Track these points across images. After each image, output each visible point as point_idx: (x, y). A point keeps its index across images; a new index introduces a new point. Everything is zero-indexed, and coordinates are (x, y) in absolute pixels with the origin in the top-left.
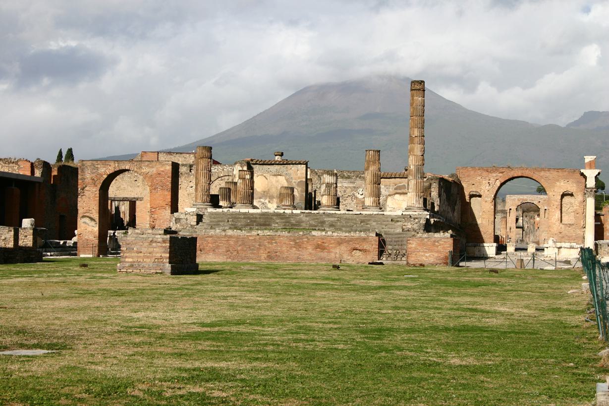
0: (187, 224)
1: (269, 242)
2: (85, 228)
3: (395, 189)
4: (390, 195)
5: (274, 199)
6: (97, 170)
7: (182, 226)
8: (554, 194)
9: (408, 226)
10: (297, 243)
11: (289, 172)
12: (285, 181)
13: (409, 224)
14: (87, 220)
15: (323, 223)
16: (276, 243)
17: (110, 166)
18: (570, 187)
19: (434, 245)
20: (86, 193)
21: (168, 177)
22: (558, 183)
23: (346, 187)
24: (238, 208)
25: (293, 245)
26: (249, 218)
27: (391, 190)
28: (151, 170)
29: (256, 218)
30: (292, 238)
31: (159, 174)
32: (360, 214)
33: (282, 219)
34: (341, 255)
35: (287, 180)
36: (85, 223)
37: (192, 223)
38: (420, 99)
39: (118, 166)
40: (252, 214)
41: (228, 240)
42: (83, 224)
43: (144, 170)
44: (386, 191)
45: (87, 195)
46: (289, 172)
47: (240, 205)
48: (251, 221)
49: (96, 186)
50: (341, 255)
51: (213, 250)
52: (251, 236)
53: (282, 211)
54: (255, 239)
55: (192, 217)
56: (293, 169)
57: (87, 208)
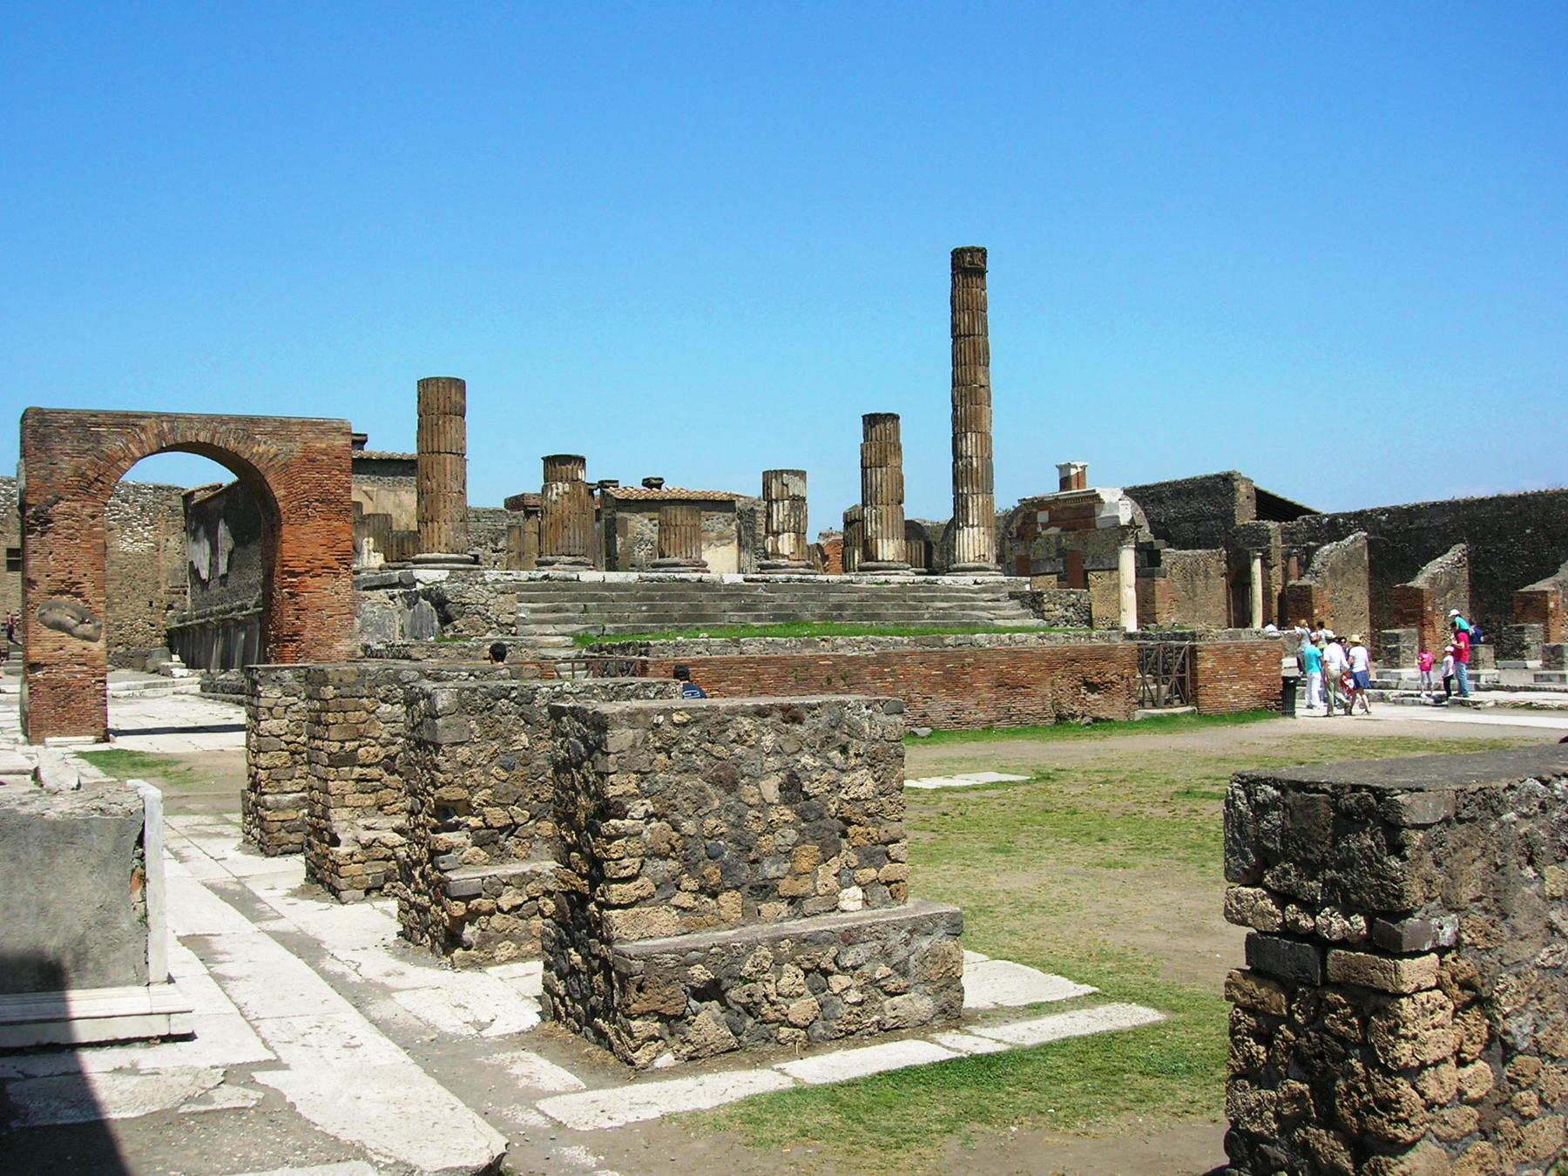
1: (873, 674)
2: (57, 645)
6: (98, 442)
10: (947, 671)
16: (893, 674)
19: (1247, 659)
20: (60, 523)
25: (939, 679)
30: (936, 659)
31: (312, 461)
34: (1056, 704)
36: (58, 626)
39: (172, 430)
50: (1056, 704)
52: (825, 657)
54: (834, 665)
55: (501, 598)
57: (63, 576)
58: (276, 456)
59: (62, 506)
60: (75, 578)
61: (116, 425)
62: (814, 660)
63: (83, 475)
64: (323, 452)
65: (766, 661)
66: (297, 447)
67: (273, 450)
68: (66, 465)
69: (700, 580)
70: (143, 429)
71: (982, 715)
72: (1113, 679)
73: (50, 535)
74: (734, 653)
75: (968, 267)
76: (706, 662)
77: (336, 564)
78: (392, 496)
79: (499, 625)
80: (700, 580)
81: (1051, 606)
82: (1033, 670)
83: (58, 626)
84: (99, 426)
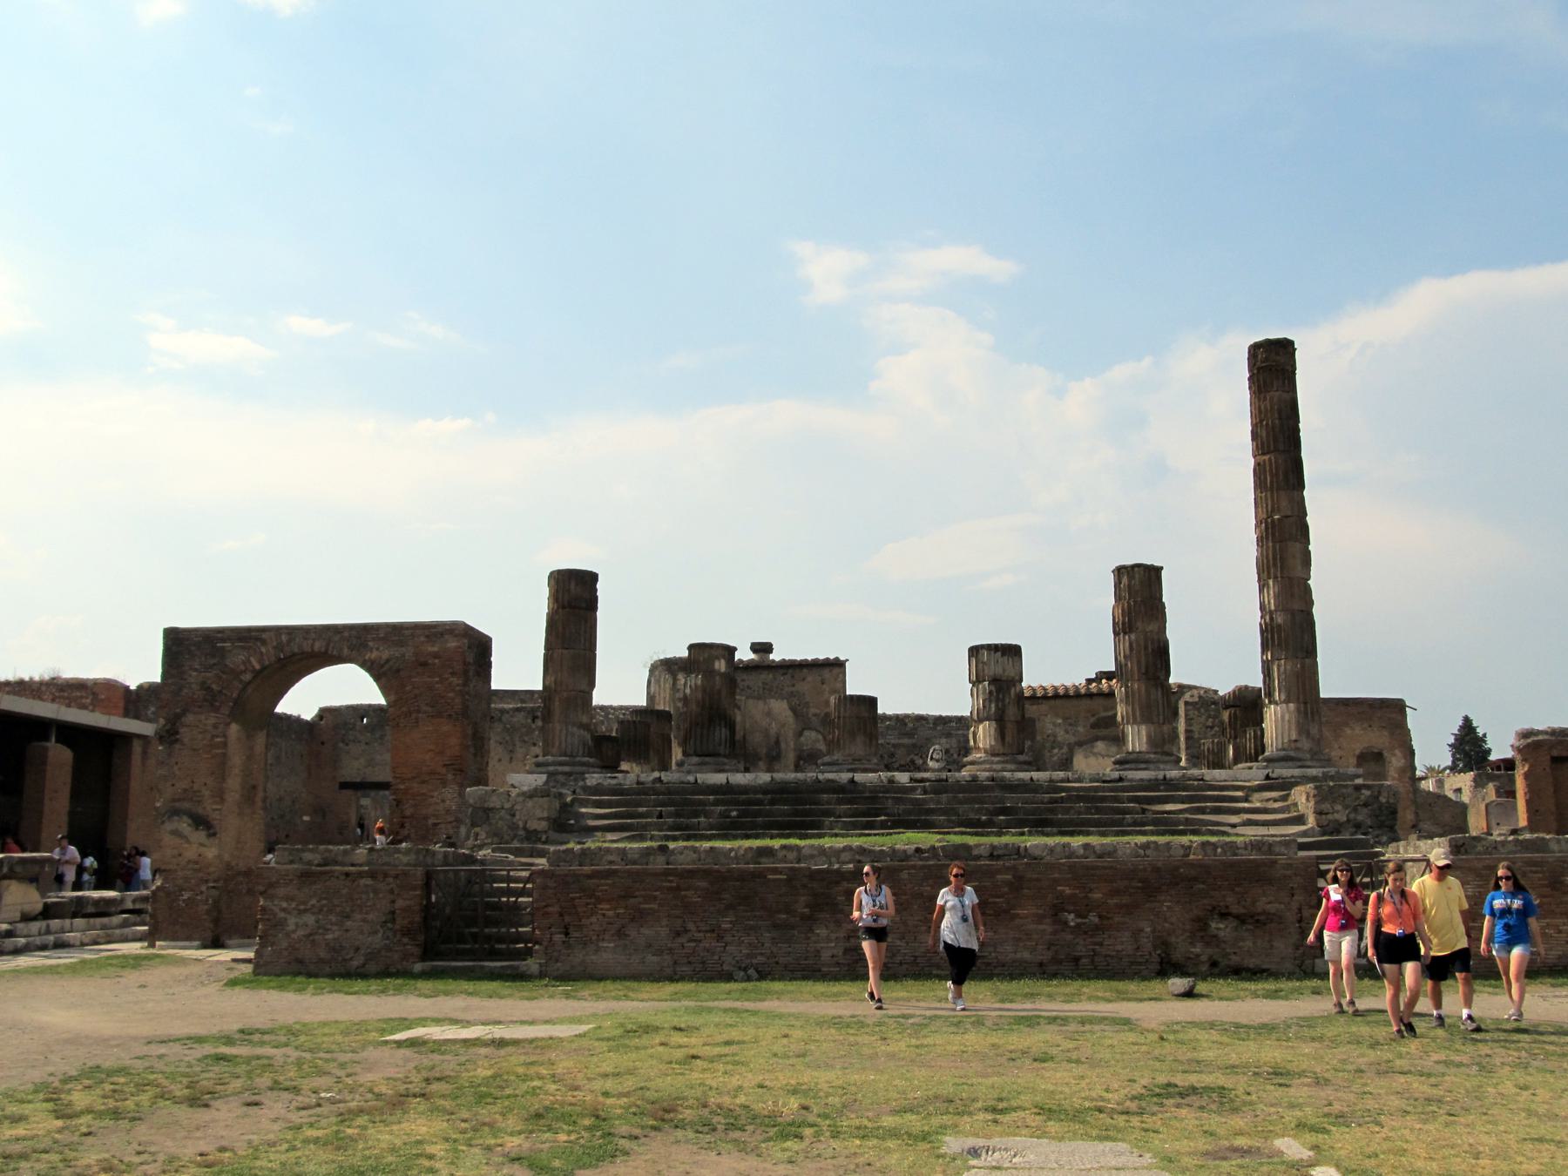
0: (514, 827)
3: (1094, 726)
4: (1080, 744)
5: (761, 764)
7: (495, 835)
8: (1340, 753)
9: (1336, 816)
11: (803, 687)
12: (789, 713)
13: (1338, 807)
14: (184, 825)
15: (1004, 811)
17: (264, 642)
18: (1375, 738)
20: (185, 734)
21: (453, 674)
22: (1349, 731)
23: (894, 746)
24: (689, 772)
26: (737, 803)
27: (1081, 729)
28: (395, 652)
29: (760, 802)
32: (1121, 779)
33: (850, 802)
35: (793, 709)
36: (176, 833)
37: (534, 825)
38: (1286, 396)
39: (289, 641)
40: (744, 790)
41: (678, 888)
42: (168, 839)
43: (374, 655)
44: (1067, 732)
45: (186, 740)
46: (803, 687)
47: (695, 759)
48: (742, 814)
49: (217, 710)
51: (620, 934)
52: (775, 871)
53: (844, 777)
54: (789, 880)
55: (530, 804)
56: (809, 679)
57: (184, 784)
58: (388, 661)
59: (190, 718)
60: (196, 787)
61: (240, 639)
62: (759, 875)
63: (209, 689)
64: (436, 656)
65: (691, 873)
66: (409, 652)
67: (385, 655)
68: (194, 678)
69: (852, 781)
70: (264, 642)
71: (1026, 955)
72: (1272, 908)
73: (177, 746)
74: (659, 863)
75: (1273, 366)
76: (610, 874)
77: (444, 771)
78: (761, 704)
79: (525, 828)
80: (852, 781)
81: (1326, 806)
82: (1116, 892)
83: (176, 833)
84: (223, 640)
